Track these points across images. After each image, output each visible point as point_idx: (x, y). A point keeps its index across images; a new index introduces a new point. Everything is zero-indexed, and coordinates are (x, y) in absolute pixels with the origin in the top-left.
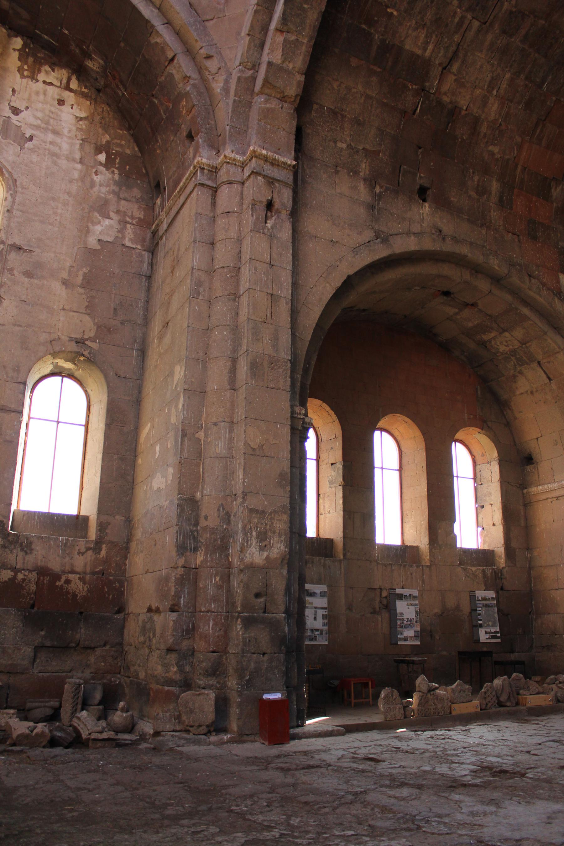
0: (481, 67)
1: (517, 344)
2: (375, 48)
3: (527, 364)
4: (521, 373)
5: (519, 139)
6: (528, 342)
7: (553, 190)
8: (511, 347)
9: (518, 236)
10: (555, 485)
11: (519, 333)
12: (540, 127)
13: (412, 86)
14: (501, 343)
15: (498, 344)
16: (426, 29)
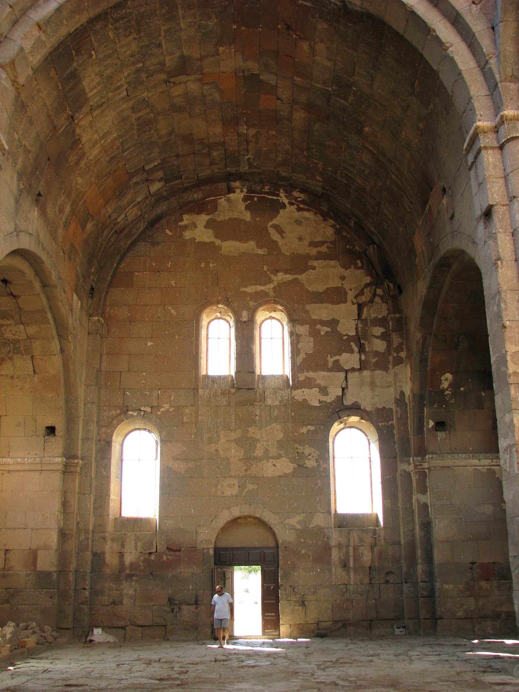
0: (108, 121)
1: (24, 336)
2: (68, 71)
3: (22, 354)
4: (11, 359)
5: (93, 180)
6: (35, 339)
7: (88, 224)
8: (17, 337)
9: (65, 254)
10: (10, 460)
11: (32, 330)
12: (106, 177)
13: (69, 111)
14: (11, 331)
15: (8, 331)
16: (101, 78)
